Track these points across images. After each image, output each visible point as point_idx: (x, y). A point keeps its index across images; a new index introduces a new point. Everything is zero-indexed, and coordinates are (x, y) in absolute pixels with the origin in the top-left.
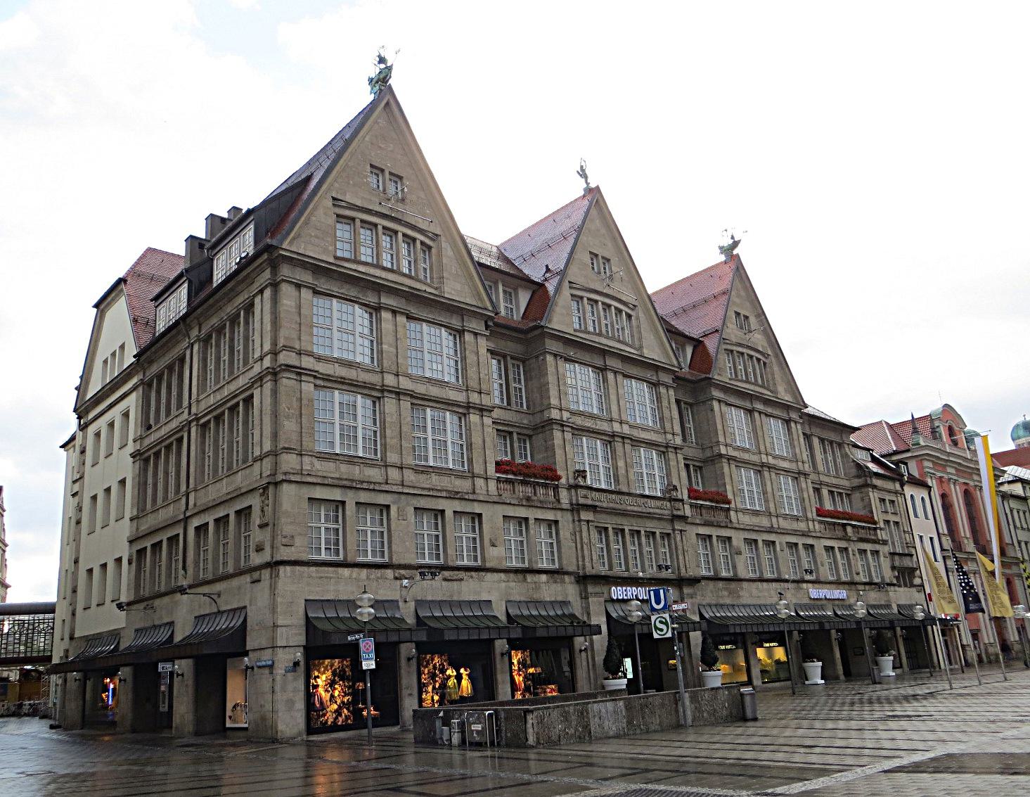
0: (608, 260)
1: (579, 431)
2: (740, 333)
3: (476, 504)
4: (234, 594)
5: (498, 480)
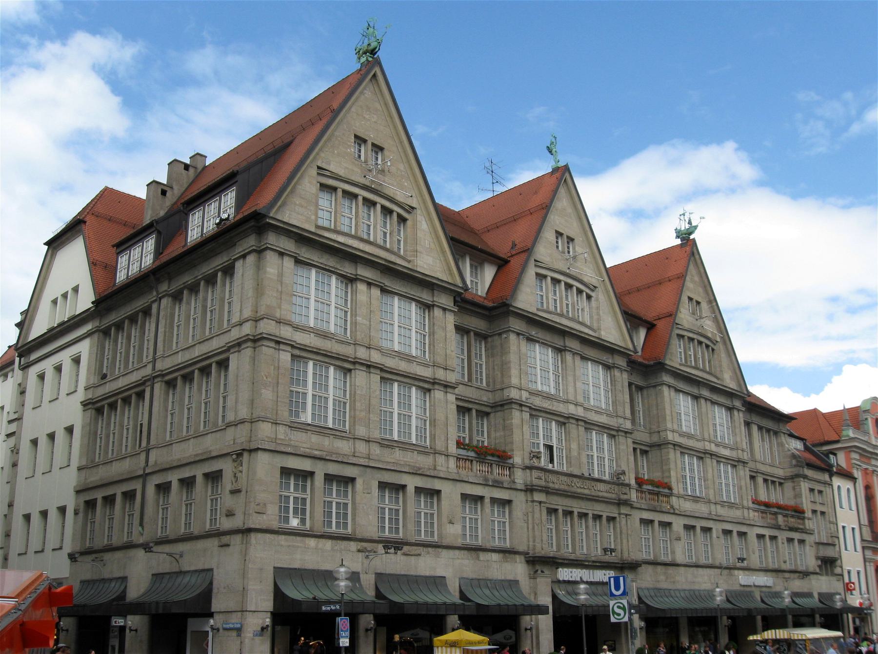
0: (572, 240)
1: (535, 412)
2: (690, 319)
3: (436, 480)
4: (197, 556)
5: (458, 459)
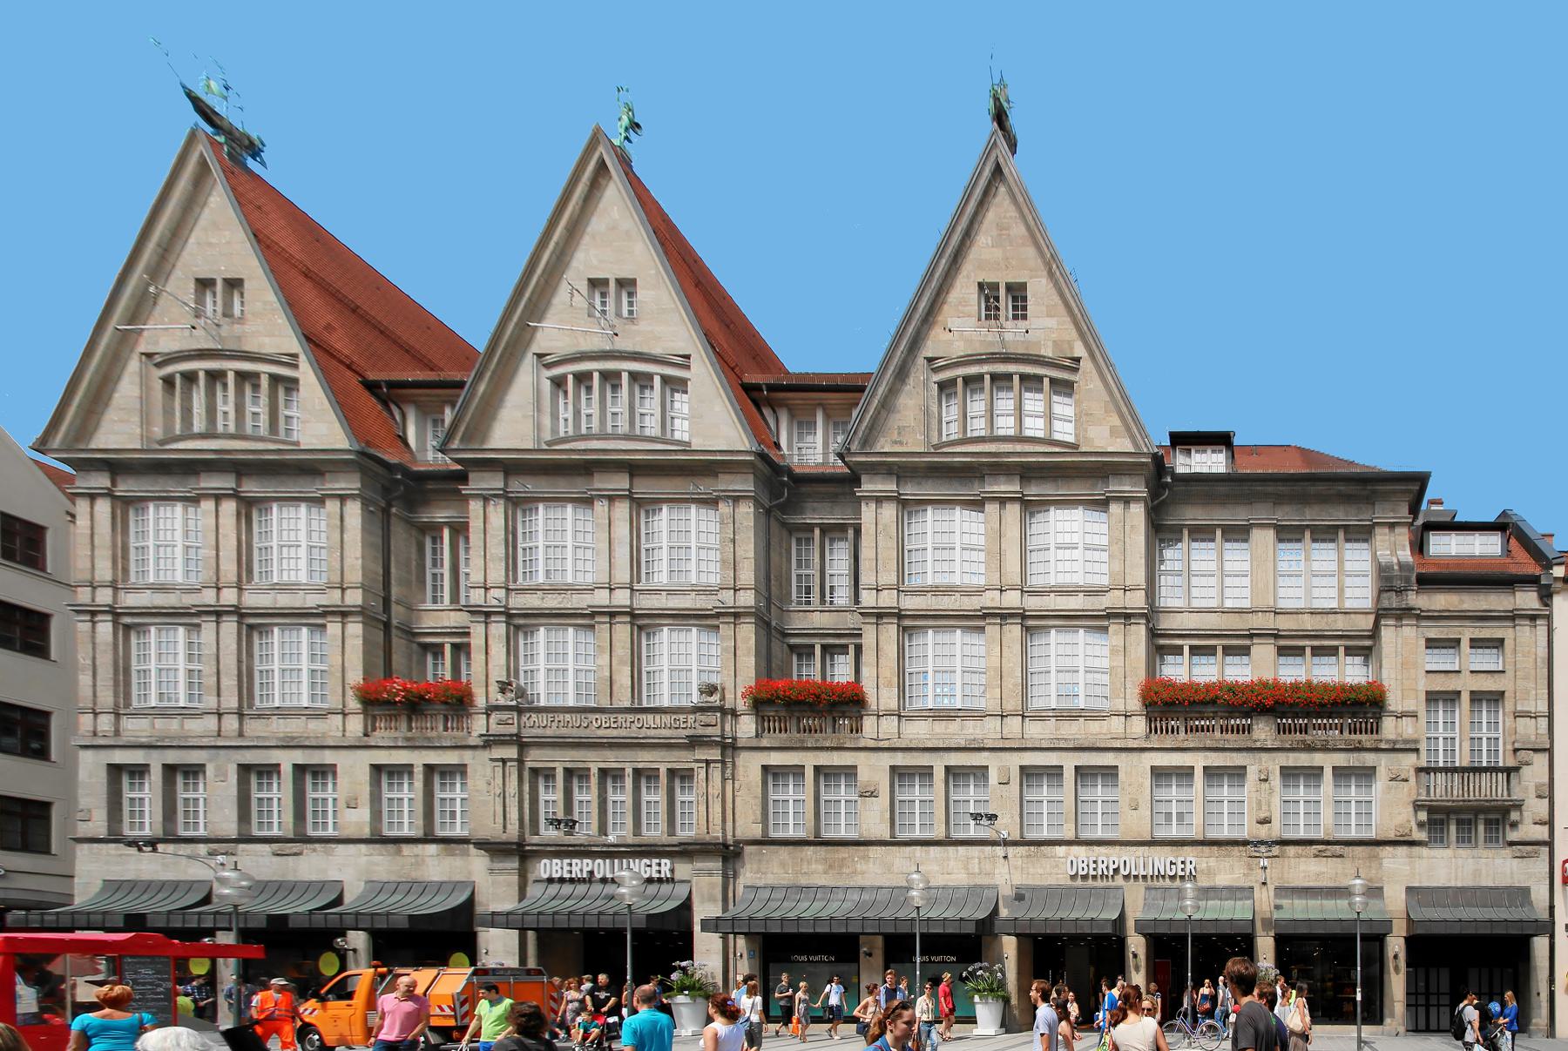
3: (327, 752)
